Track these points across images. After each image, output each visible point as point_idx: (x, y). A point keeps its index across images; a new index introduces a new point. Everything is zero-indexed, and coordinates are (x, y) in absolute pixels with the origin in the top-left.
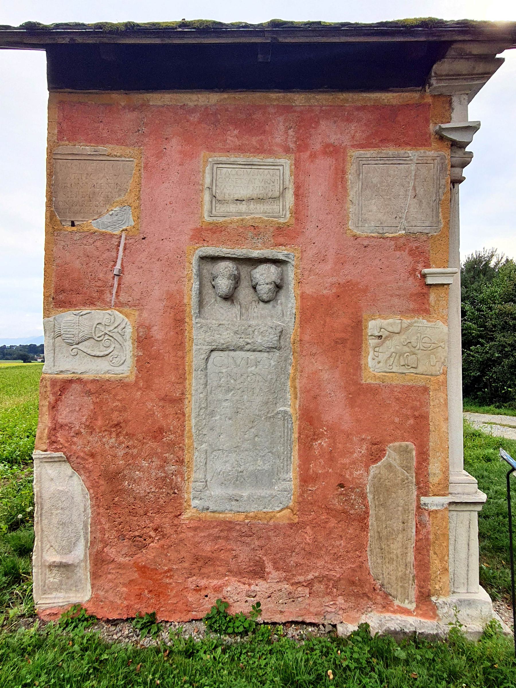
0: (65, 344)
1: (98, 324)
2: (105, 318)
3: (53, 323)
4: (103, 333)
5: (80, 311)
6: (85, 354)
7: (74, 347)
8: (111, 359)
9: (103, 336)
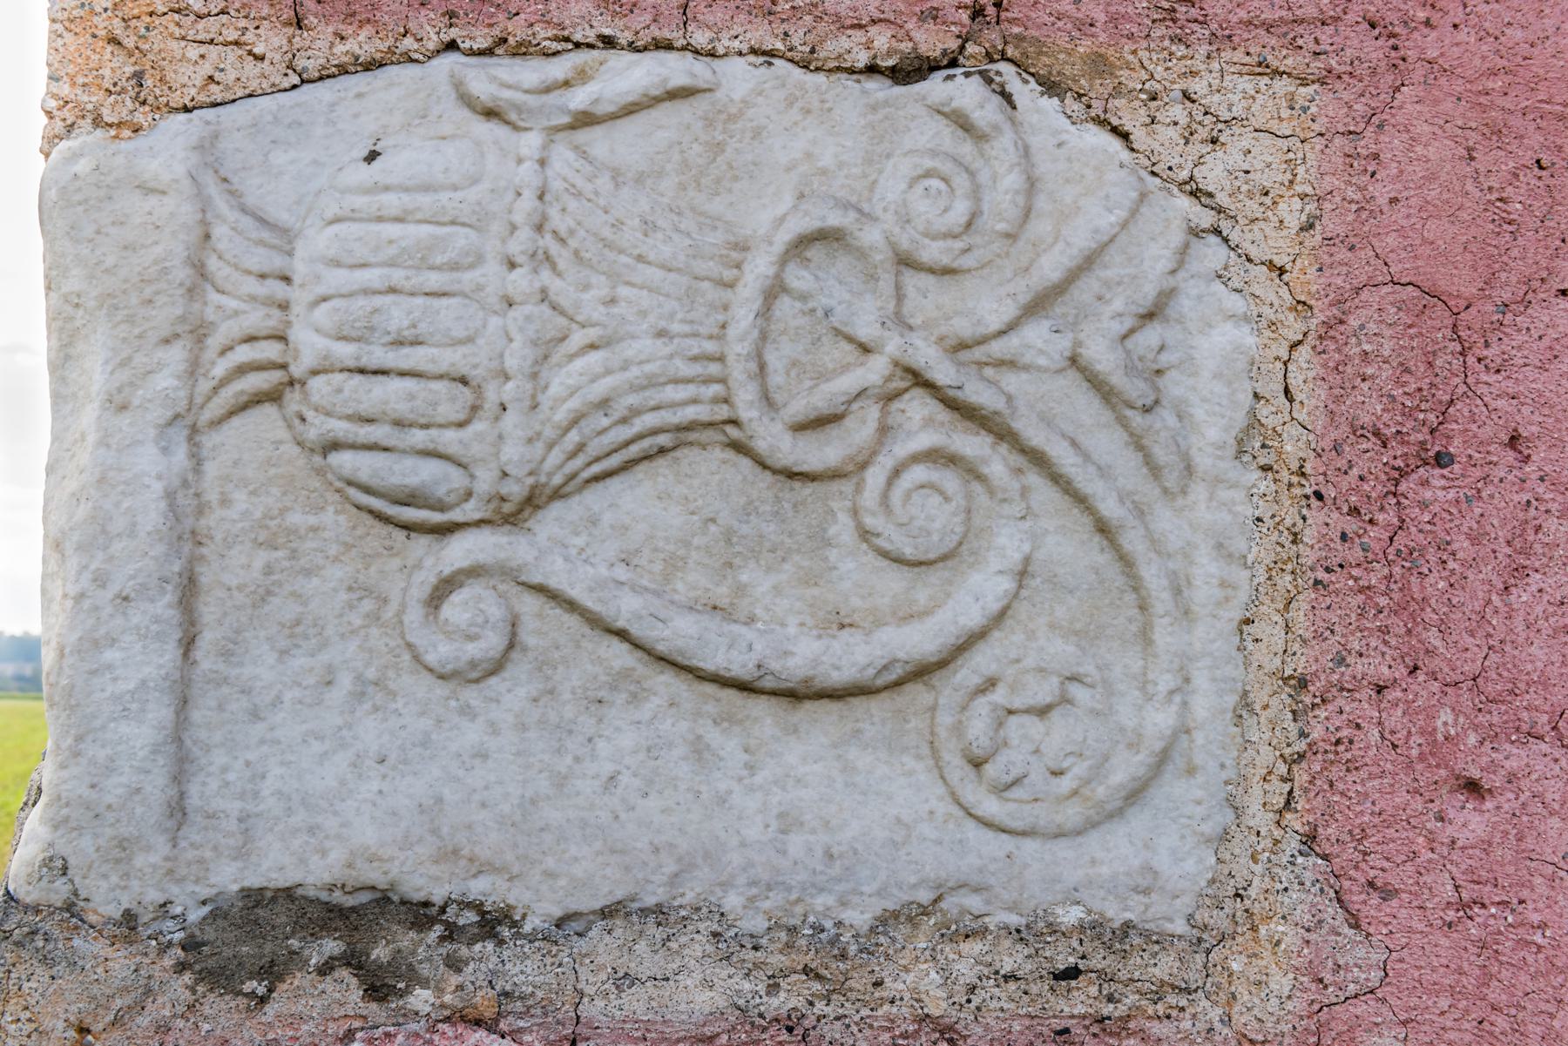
0: (335, 520)
1: (803, 244)
3: (187, 212)
4: (874, 371)
5: (558, 68)
6: (619, 655)
7: (460, 551)
8: (978, 728)
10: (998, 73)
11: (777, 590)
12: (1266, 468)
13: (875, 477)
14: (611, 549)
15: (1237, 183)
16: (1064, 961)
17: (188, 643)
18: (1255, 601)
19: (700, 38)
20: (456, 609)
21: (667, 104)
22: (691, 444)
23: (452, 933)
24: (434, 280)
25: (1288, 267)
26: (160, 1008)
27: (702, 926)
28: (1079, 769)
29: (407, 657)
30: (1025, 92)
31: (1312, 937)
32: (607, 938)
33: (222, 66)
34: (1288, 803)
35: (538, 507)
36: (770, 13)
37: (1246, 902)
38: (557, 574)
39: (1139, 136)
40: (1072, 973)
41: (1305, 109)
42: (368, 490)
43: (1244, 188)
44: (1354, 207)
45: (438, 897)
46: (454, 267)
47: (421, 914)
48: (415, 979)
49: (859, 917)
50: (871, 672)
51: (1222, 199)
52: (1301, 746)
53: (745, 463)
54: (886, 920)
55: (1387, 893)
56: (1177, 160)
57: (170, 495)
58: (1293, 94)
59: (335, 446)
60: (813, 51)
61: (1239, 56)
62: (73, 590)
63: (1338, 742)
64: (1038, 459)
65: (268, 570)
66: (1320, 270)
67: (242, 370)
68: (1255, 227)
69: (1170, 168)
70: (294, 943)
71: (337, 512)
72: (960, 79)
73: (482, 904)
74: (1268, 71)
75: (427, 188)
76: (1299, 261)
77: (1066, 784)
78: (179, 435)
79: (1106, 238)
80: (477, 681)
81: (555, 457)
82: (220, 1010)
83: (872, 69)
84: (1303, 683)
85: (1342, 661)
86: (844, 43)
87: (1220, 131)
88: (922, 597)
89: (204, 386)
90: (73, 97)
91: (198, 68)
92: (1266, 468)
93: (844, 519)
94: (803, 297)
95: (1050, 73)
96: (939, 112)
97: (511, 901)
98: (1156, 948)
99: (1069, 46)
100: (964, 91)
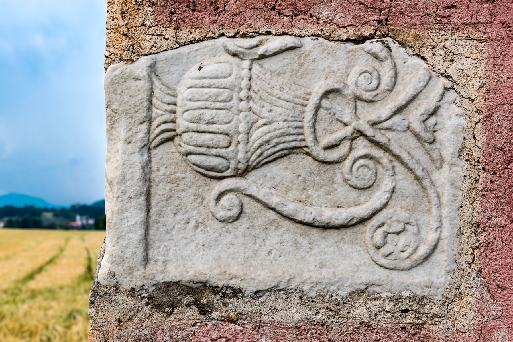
0: (190, 175)
1: (326, 94)
2: (357, 69)
3: (147, 86)
4: (348, 131)
6: (272, 215)
7: (226, 184)
8: (378, 238)
9: (347, 144)
10: (386, 41)
11: (319, 196)
12: (467, 161)
13: (348, 163)
14: (270, 184)
15: (460, 74)
16: (404, 306)
17: (148, 211)
18: (464, 200)
19: (297, 32)
20: (225, 201)
21: (287, 52)
22: (294, 153)
23: (224, 295)
24: (219, 105)
25: (475, 99)
26: (141, 315)
27: (297, 295)
28: (409, 250)
29: (211, 215)
30: (395, 46)
31: (480, 301)
32: (269, 298)
33: (156, 42)
34: (473, 261)
35: (248, 172)
36: (317, 23)
37: (460, 290)
38: (253, 190)
39: (429, 59)
40: (407, 311)
41: (481, 50)
42: (199, 166)
43: (462, 75)
44: (496, 81)
45: (220, 285)
46: (225, 101)
47: (215, 290)
48: (214, 308)
49: (343, 293)
50: (347, 221)
51: (455, 79)
52: (477, 244)
53: (310, 159)
54: (352, 294)
55: (503, 289)
56: (441, 67)
57: (143, 168)
58: (477, 46)
60: (330, 35)
61: (461, 34)
62: (116, 195)
63: (489, 243)
64: (398, 158)
66: (485, 100)
67: (163, 131)
68: (465, 87)
69: (439, 69)
70: (179, 298)
71: (190, 173)
72: (375, 43)
73: (233, 287)
74: (470, 39)
75: (216, 78)
76: (478, 98)
77: (405, 254)
78: (145, 150)
79: (419, 91)
80: (231, 222)
81: (254, 157)
82: (158, 317)
83: (348, 40)
84: (478, 226)
85: (490, 219)
86: (340, 32)
87: (455, 57)
88: (362, 199)
89: (152, 136)
90: (114, 52)
91: (149, 43)
92: (467, 161)
93: (339, 175)
94: (327, 109)
95: (402, 40)
96: (368, 53)
97: (241, 287)
98: (432, 304)
99: (408, 32)
100: (375, 46)
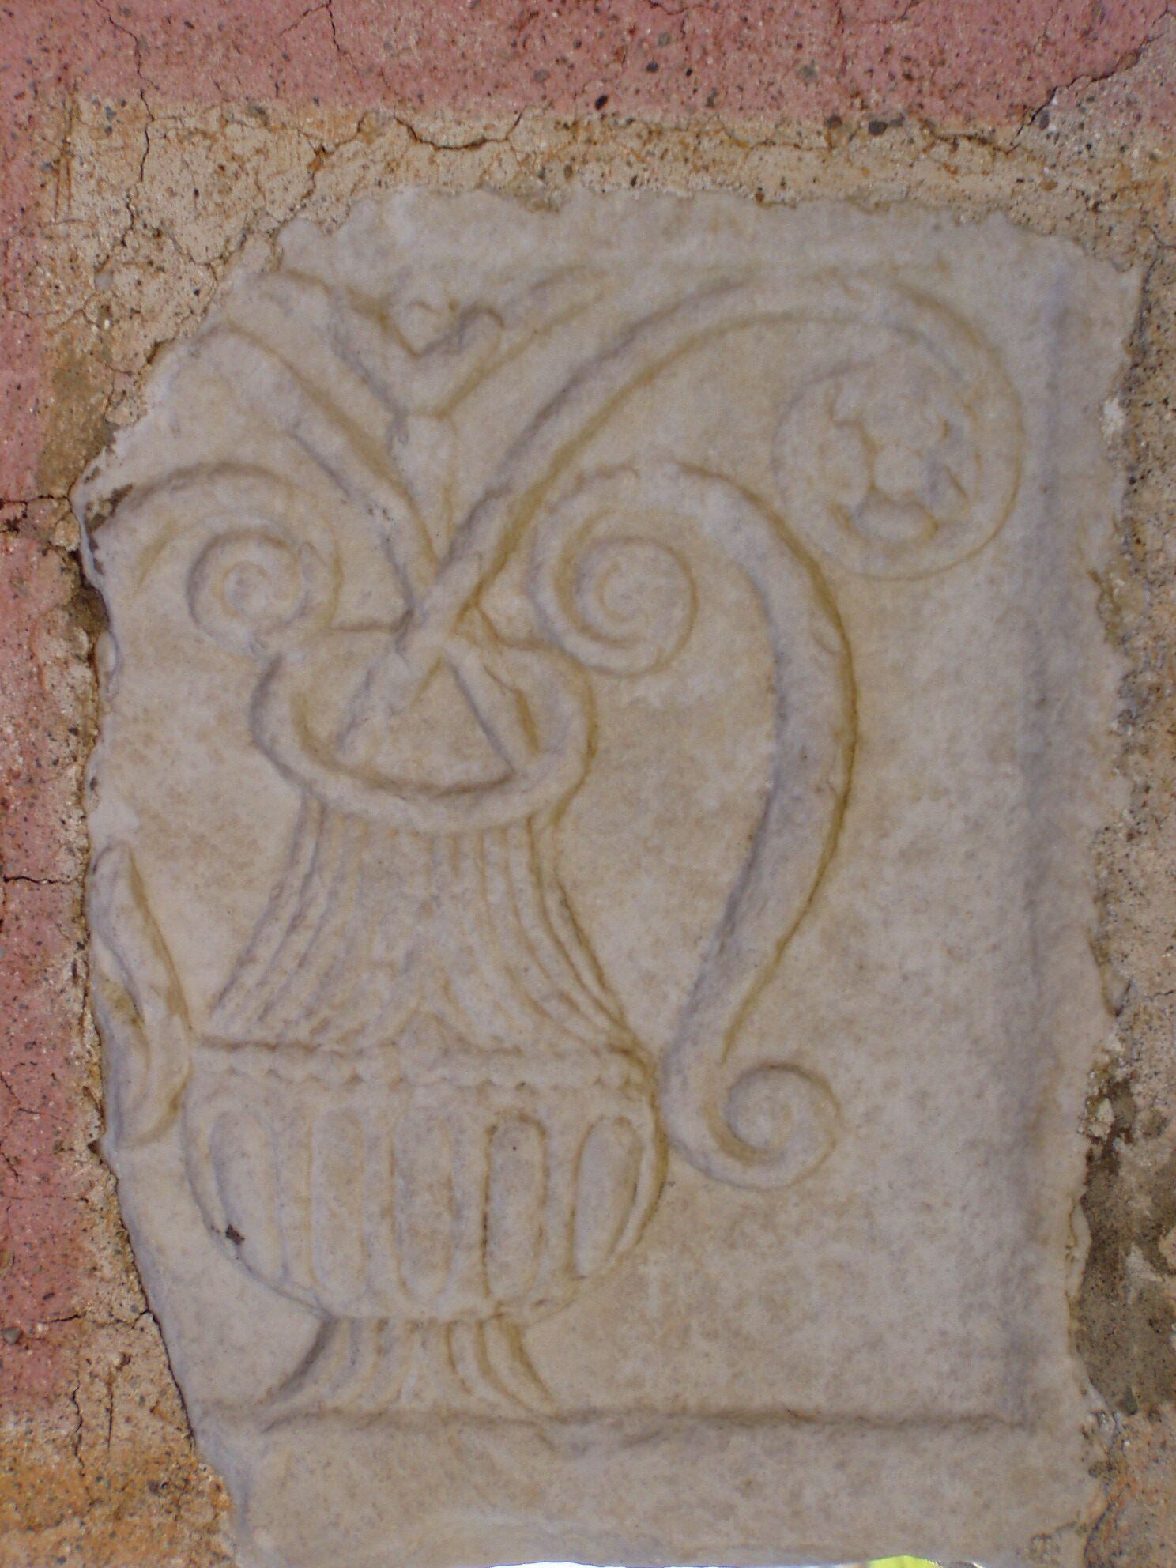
10: (89, 507)
12: (569, 171)
13: (588, 651)
15: (211, 208)
19: (68, 865)
21: (151, 903)
22: (556, 869)
23: (1122, 1130)
25: (316, 145)
27: (1120, 852)
29: (809, 1183)
31: (1147, 113)
32: (1132, 958)
33: (137, 1398)
34: (983, 142)
35: (636, 1043)
36: (30, 781)
37: (1105, 196)
39: (155, 332)
41: (110, 114)
42: (620, 1231)
43: (217, 198)
44: (234, 54)
50: (824, 658)
51: (233, 226)
53: (578, 803)
56: (185, 283)
58: (91, 129)
59: (570, 1269)
60: (74, 731)
61: (48, 199)
63: (908, 77)
65: (711, 1336)
66: (317, 101)
67: (487, 1371)
68: (267, 186)
69: (197, 293)
70: (1132, 1296)
71: (645, 1261)
72: (101, 555)
73: (1090, 1098)
74: (63, 161)
76: (307, 129)
79: (288, 376)
80: (838, 1106)
84: (834, 121)
85: (808, 73)
87: (145, 226)
90: (185, 1554)
91: (143, 1424)
92: (569, 171)
95: (84, 441)
96: (142, 579)
97: (1087, 1066)
98: (1155, 311)
99: (47, 417)
